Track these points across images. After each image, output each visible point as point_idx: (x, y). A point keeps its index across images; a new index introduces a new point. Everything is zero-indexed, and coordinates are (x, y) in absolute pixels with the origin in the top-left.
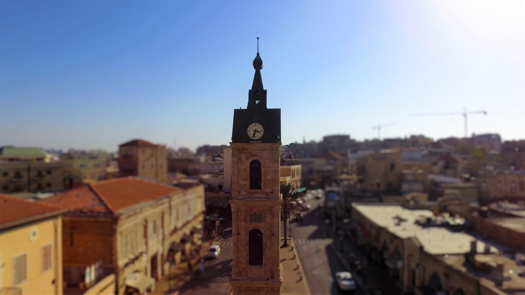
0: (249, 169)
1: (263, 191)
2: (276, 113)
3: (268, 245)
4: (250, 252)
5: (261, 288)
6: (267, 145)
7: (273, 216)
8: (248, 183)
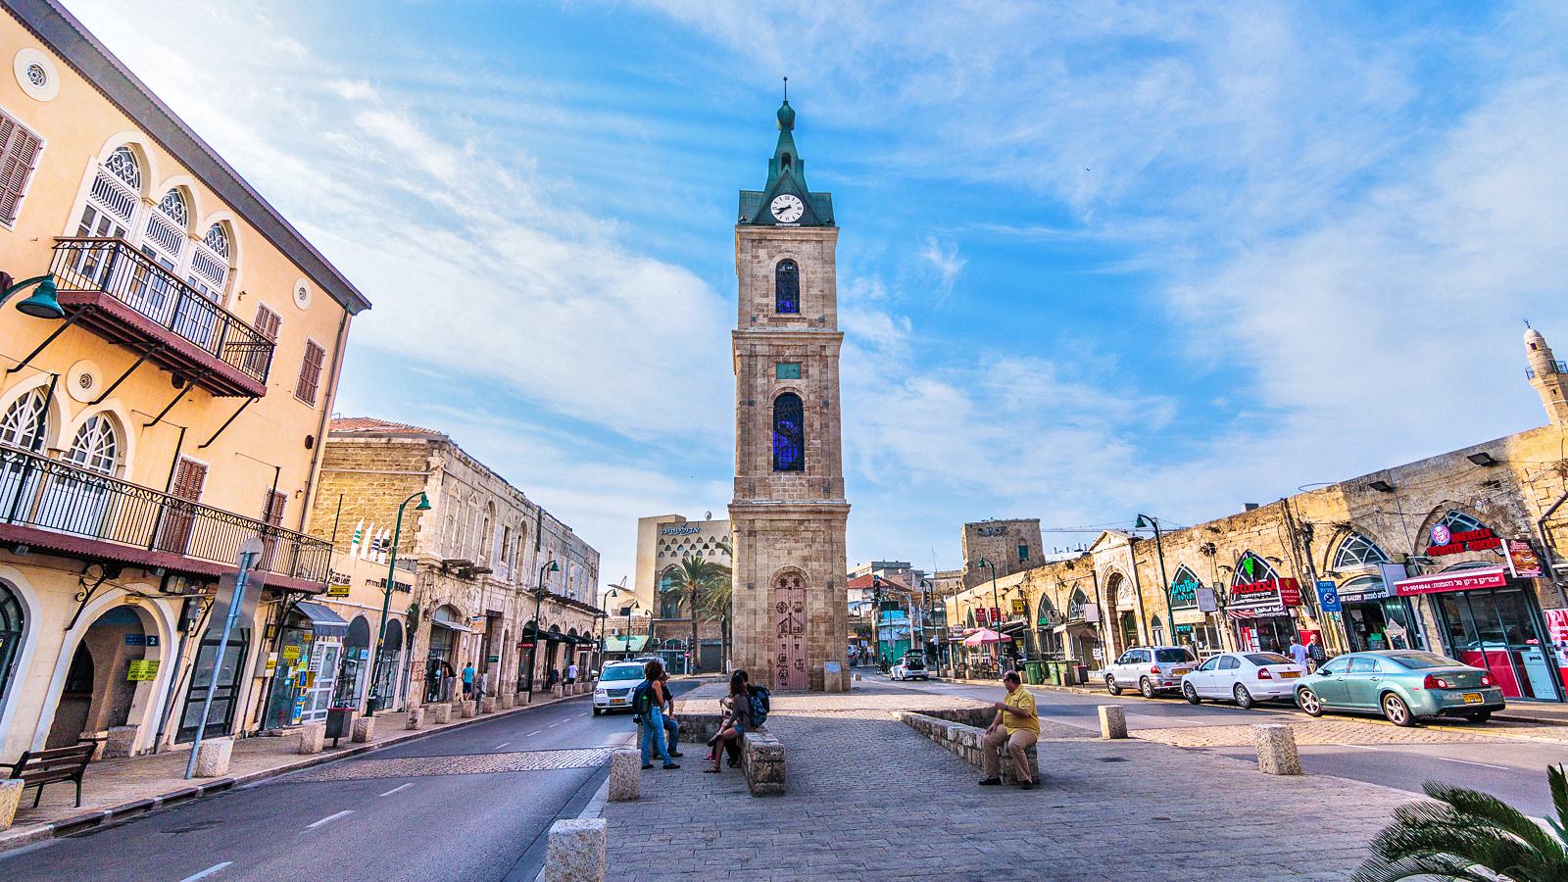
1: (802, 316)
3: (817, 425)
5: (801, 522)
6: (812, 232)
8: (772, 301)
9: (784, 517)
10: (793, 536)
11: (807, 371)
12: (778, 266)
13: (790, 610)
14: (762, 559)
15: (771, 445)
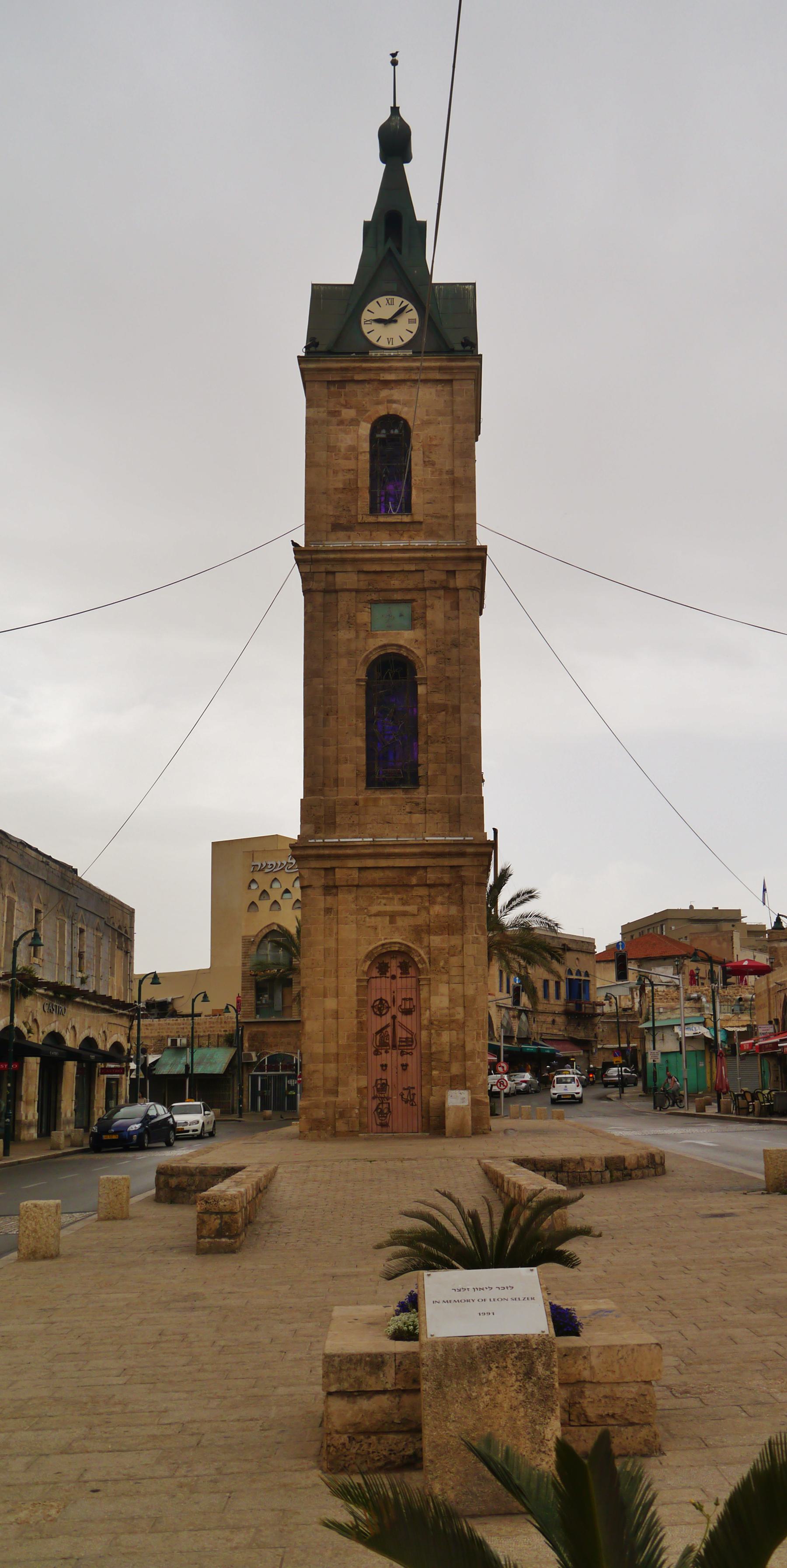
0: (366, 446)
1: (418, 518)
2: (462, 298)
4: (370, 737)
7: (456, 606)
9: (383, 863)
10: (398, 893)
11: (424, 616)
12: (374, 430)
13: (394, 1011)
14: (348, 932)
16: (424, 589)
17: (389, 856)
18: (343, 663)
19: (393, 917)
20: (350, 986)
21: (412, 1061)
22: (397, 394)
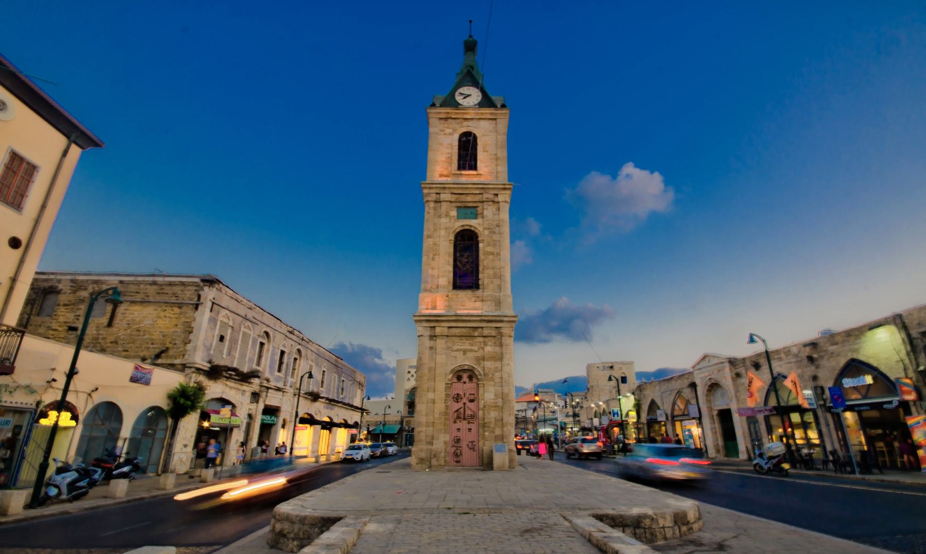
0: (456, 143)
4: (455, 266)
6: (487, 111)
11: (482, 213)
13: (464, 400)
15: (451, 269)
16: (483, 202)
17: (464, 321)
18: (443, 233)
19: (465, 352)
20: (441, 386)
21: (473, 427)
22: (470, 123)
